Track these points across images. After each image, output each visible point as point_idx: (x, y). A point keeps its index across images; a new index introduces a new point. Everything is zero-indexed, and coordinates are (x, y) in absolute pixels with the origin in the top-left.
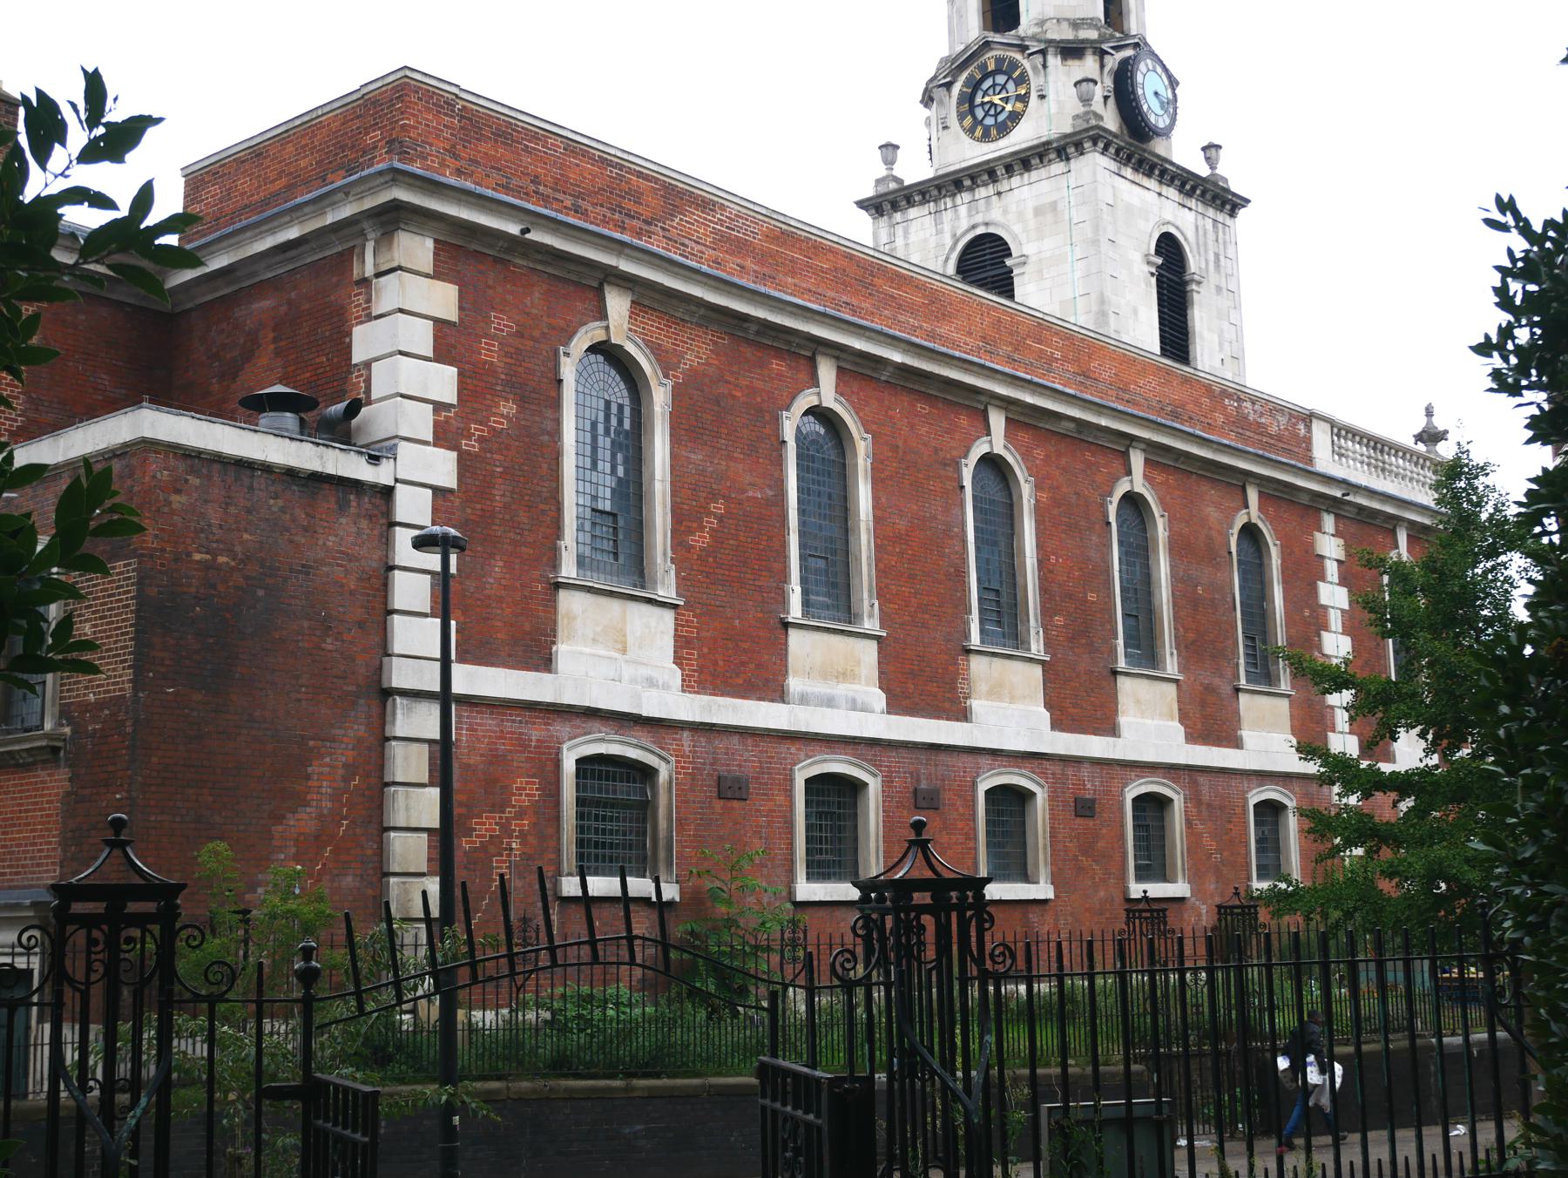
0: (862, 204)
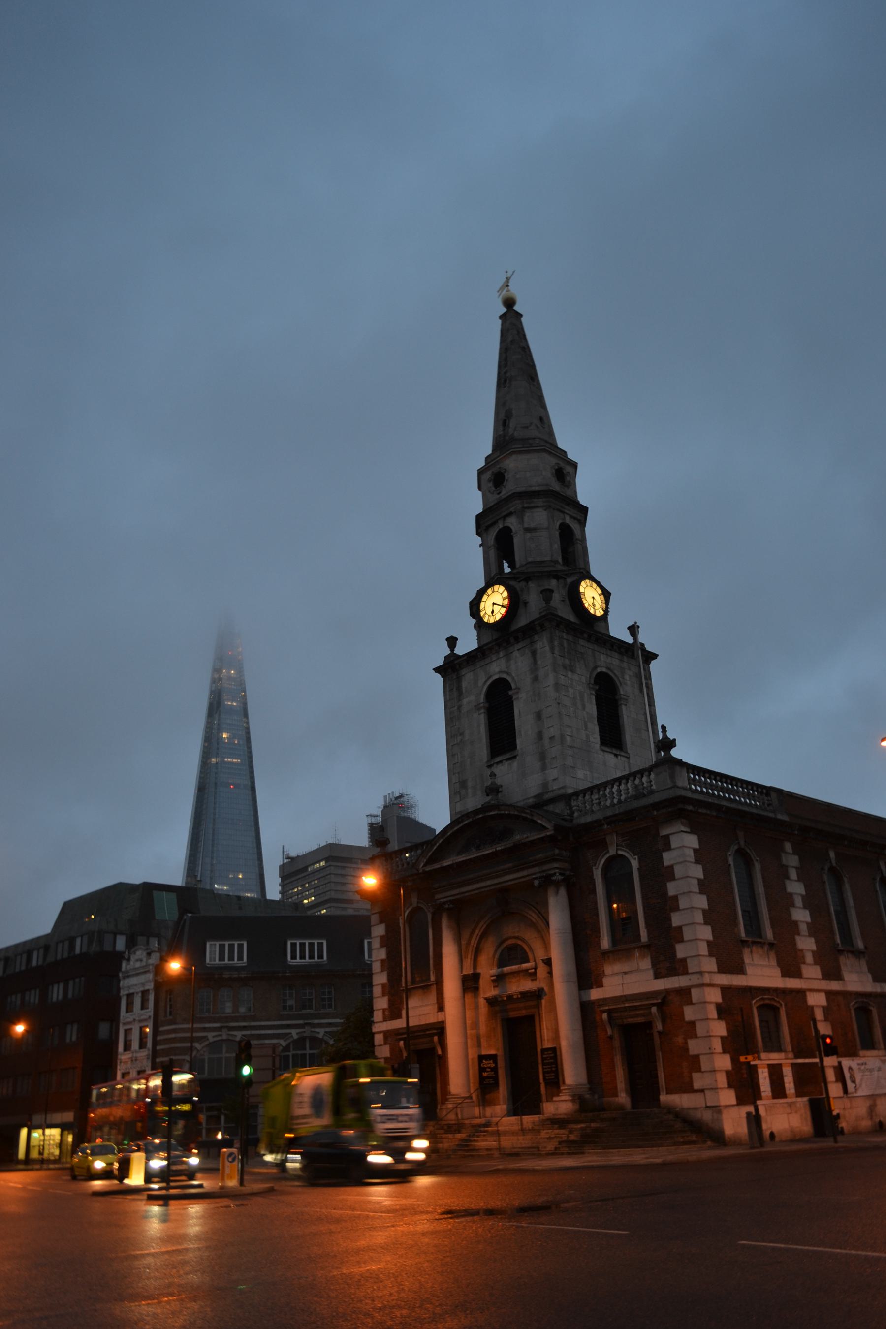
0: (437, 670)
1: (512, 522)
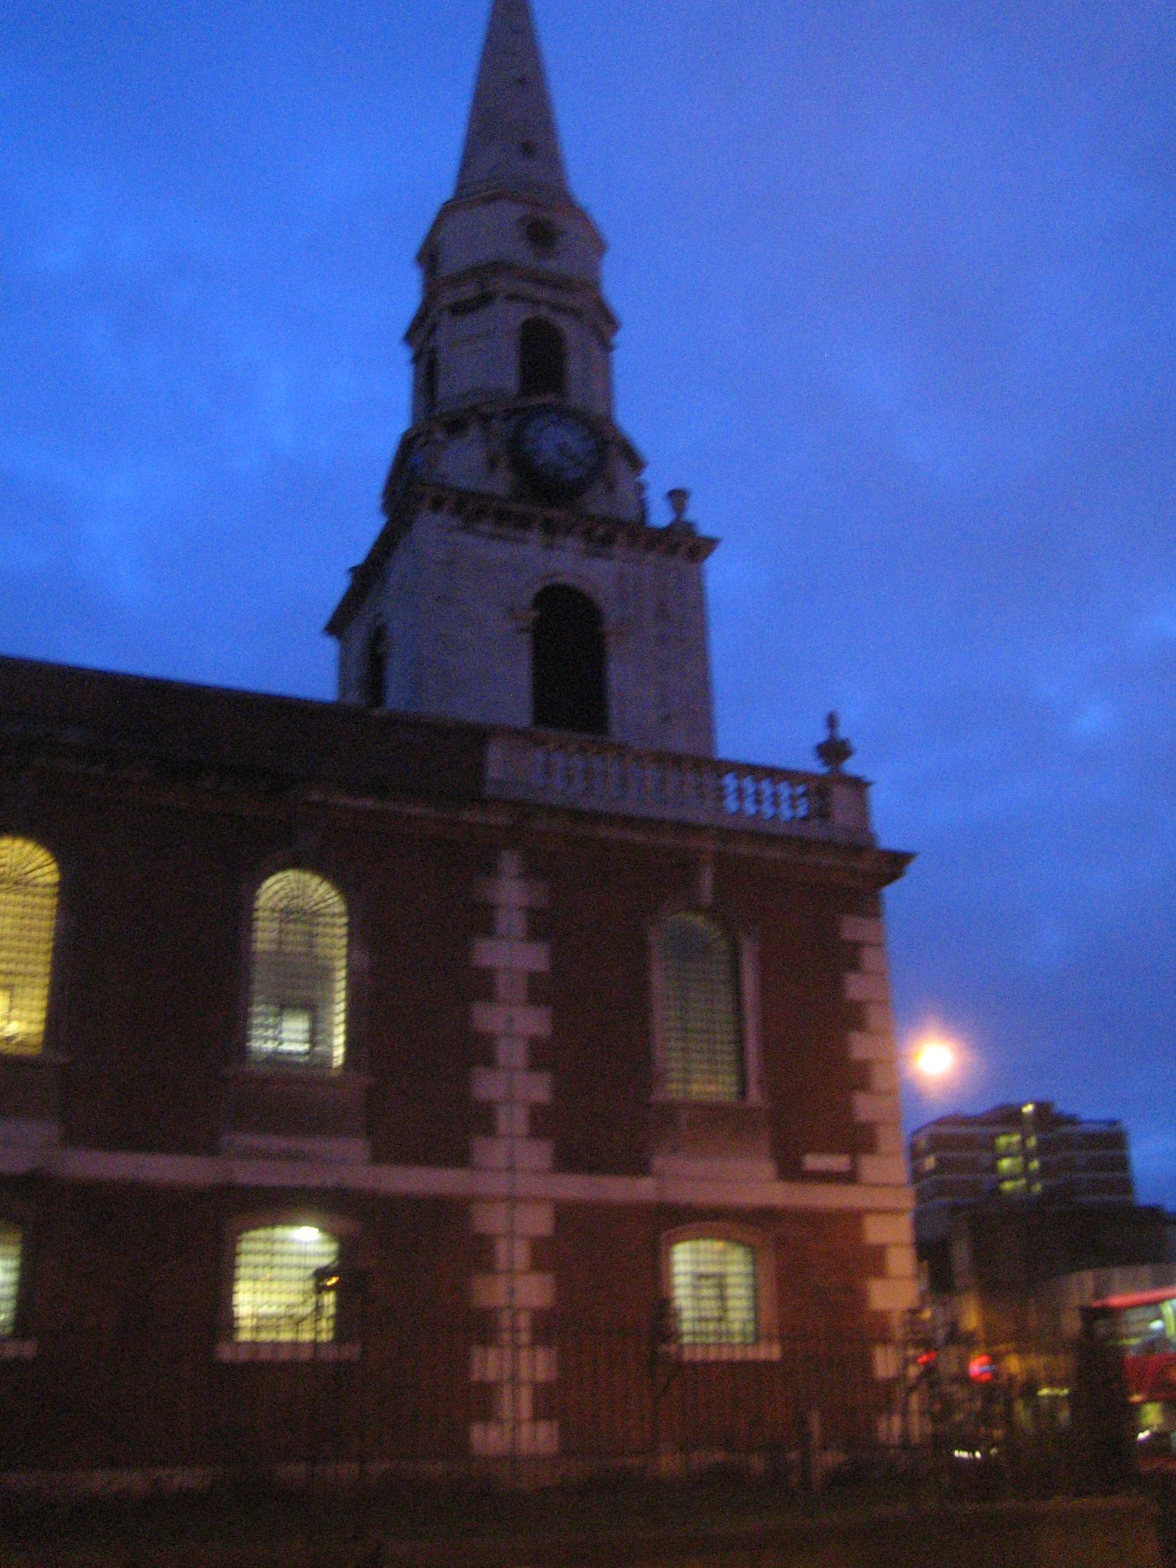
1: (564, 324)
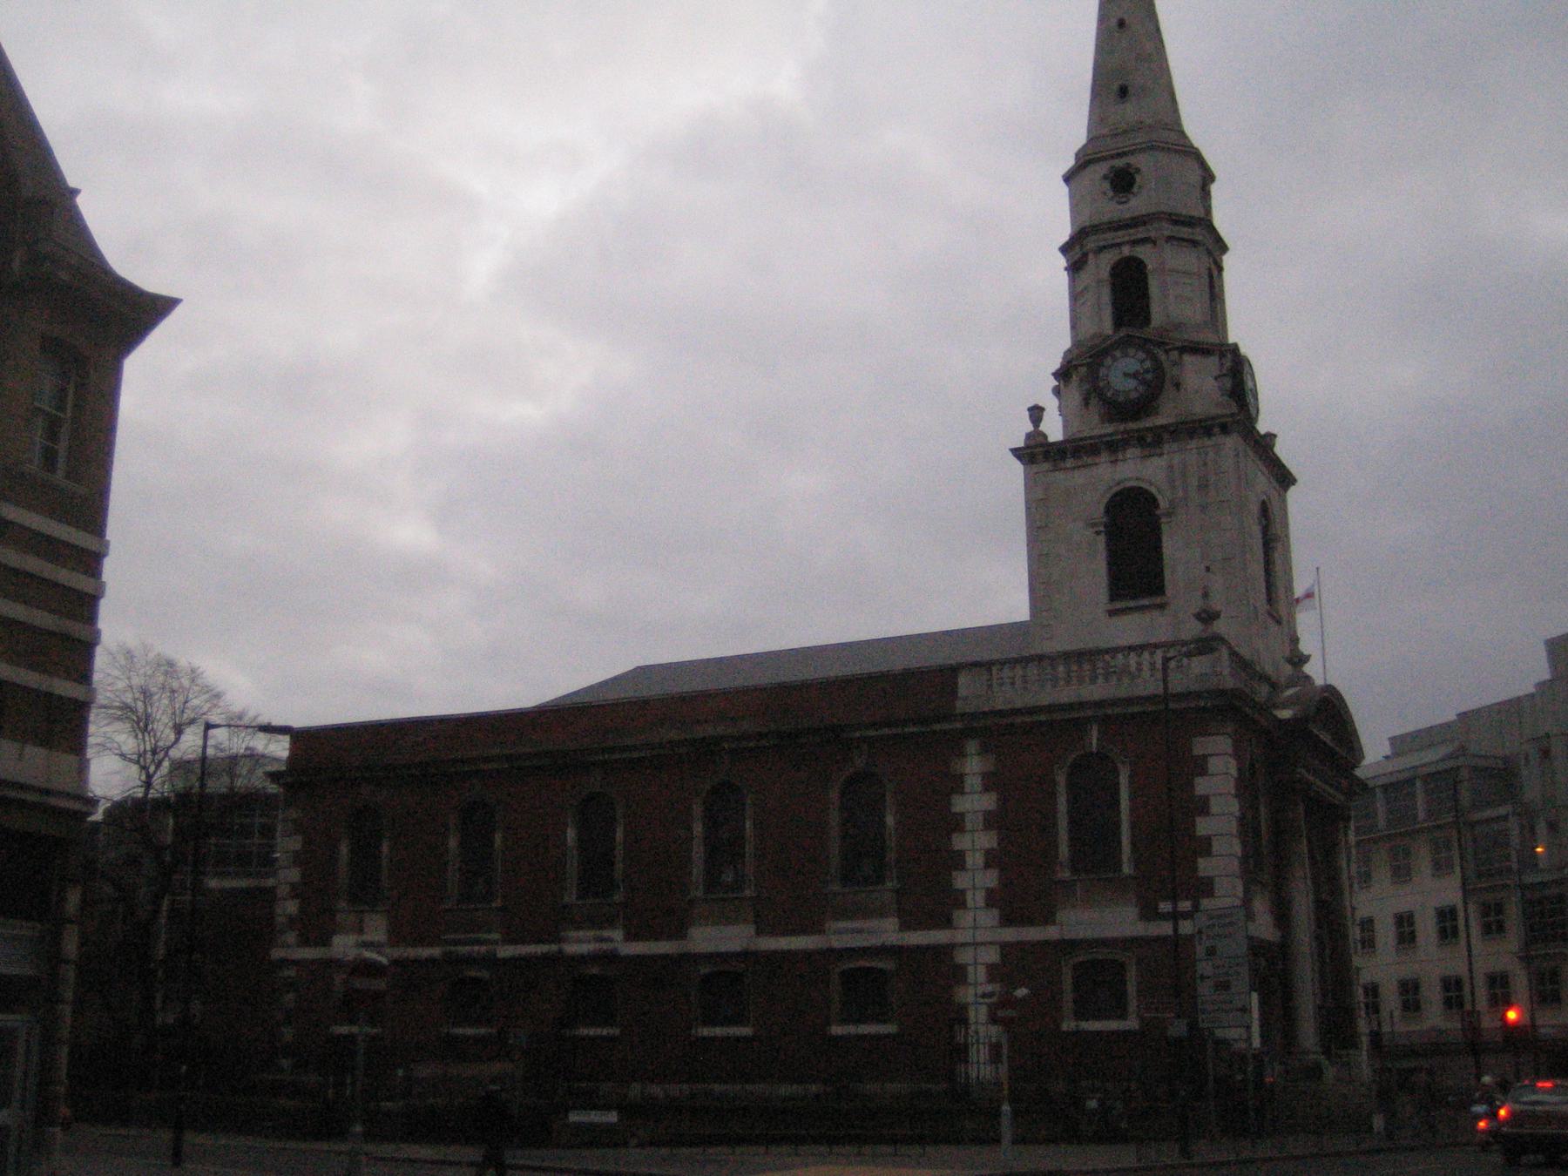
0: (1017, 452)
1: (1142, 252)
